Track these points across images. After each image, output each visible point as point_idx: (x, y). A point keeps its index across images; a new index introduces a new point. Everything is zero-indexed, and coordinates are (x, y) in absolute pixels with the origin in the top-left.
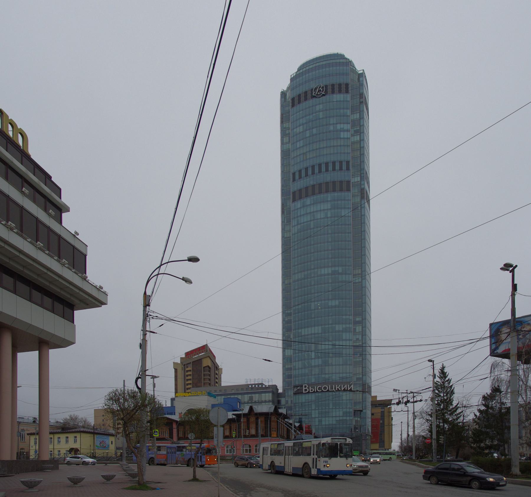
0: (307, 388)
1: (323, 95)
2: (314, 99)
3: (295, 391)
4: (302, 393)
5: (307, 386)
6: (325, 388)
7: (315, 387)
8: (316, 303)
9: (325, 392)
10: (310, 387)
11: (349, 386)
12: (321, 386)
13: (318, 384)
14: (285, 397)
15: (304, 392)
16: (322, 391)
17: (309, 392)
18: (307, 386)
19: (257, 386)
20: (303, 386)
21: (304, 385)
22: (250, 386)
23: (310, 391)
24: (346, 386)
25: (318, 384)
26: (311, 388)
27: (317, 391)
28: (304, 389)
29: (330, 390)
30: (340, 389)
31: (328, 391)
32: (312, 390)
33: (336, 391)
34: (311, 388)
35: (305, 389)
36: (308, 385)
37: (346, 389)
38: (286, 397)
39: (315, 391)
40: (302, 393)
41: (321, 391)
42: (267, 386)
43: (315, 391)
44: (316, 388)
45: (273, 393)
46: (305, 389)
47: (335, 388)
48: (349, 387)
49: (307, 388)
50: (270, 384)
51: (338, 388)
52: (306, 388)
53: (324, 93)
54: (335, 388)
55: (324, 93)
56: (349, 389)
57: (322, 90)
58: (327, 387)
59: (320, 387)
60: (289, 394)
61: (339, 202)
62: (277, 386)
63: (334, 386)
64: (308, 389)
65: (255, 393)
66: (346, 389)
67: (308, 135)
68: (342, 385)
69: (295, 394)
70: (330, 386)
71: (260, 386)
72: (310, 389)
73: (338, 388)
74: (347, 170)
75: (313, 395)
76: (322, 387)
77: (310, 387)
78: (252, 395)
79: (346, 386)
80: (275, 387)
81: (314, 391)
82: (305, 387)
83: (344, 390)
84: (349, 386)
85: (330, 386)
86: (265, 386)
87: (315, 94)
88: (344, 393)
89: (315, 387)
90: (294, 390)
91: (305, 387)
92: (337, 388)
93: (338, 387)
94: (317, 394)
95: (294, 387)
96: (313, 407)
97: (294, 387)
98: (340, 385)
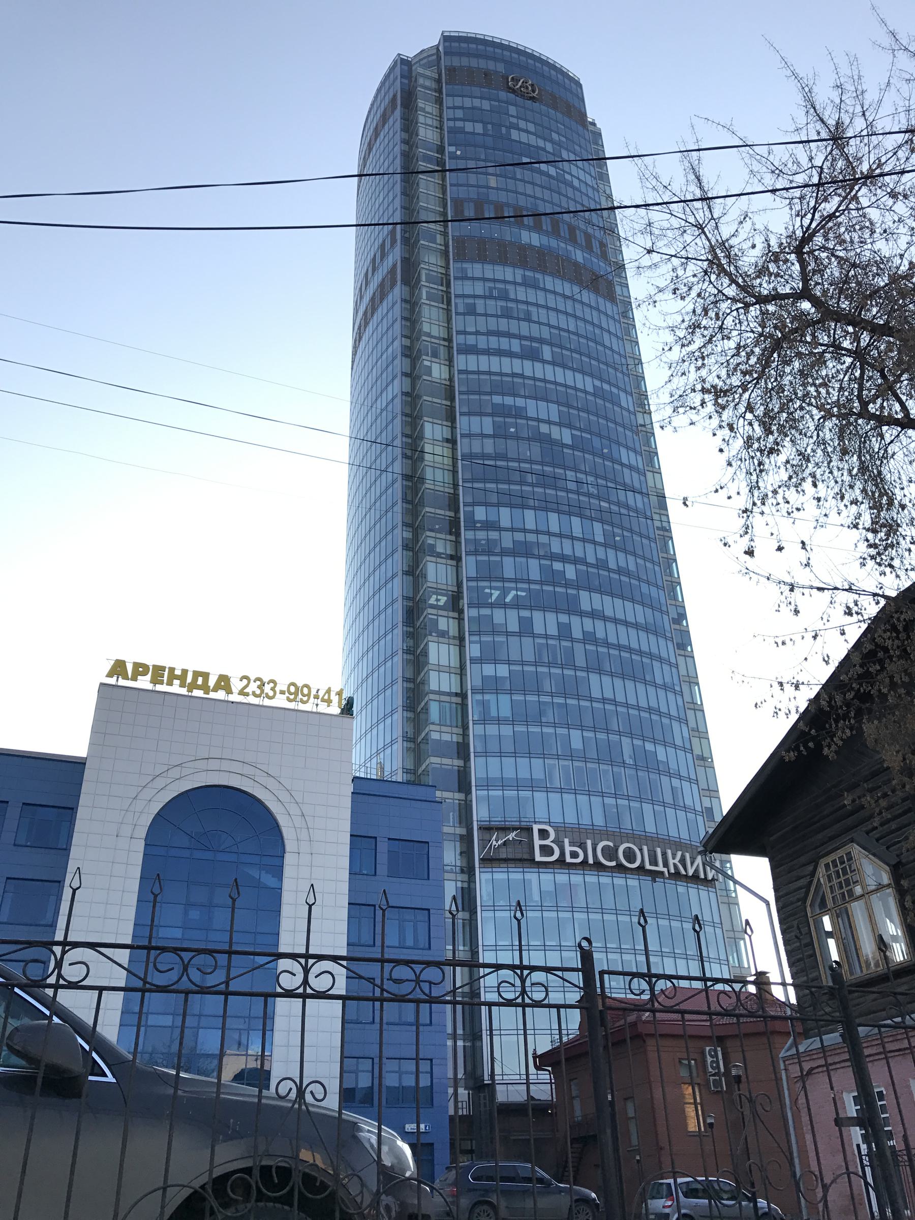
5: (552, 835)
7: (589, 843)
9: (631, 869)
10: (566, 841)
12: (611, 844)
15: (538, 858)
18: (552, 835)
21: (536, 828)
23: (569, 859)
28: (537, 842)
31: (641, 868)
32: (574, 855)
35: (541, 847)
39: (591, 861)
40: (530, 862)
41: (613, 864)
43: (591, 861)
44: (596, 850)
46: (541, 847)
47: (666, 864)
54: (666, 864)
63: (659, 851)
68: (688, 856)
70: (645, 848)
72: (568, 849)
77: (566, 841)
81: (585, 862)
82: (543, 834)
85: (645, 848)
89: (589, 843)
91: (543, 834)
92: (671, 862)
93: (674, 859)
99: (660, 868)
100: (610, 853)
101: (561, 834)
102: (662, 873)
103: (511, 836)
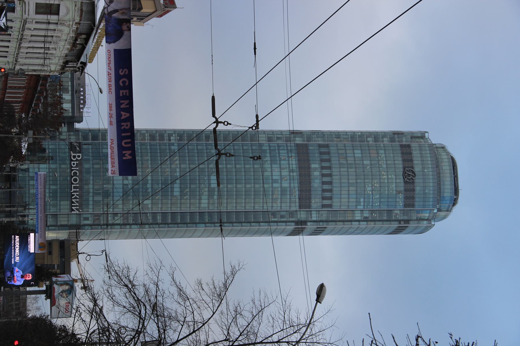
1: (404, 179)
2: (402, 170)
7: (77, 168)
10: (77, 162)
11: (78, 207)
12: (78, 175)
13: (80, 172)
14: (69, 131)
16: (72, 177)
19: (82, 97)
20: (80, 153)
21: (80, 155)
22: (82, 89)
23: (72, 162)
24: (77, 204)
29: (73, 185)
30: (73, 197)
34: (76, 163)
36: (80, 160)
37: (73, 205)
38: (68, 133)
39: (72, 168)
41: (72, 175)
42: (82, 110)
43: (72, 168)
45: (73, 117)
47: (74, 192)
48: (76, 208)
49: (77, 159)
50: (85, 114)
51: (75, 195)
53: (406, 181)
54: (74, 192)
55: (406, 181)
56: (73, 208)
57: (410, 178)
58: (77, 182)
59: (77, 173)
60: (72, 137)
61: (288, 197)
62: (82, 122)
63: (78, 190)
64: (75, 159)
65: (72, 96)
66: (73, 205)
67: (365, 162)
69: (71, 143)
71: (82, 102)
72: (75, 162)
73: (74, 195)
74: (323, 205)
75: (68, 166)
76: (77, 176)
77: (77, 162)
78: (70, 92)
79: (77, 204)
80: (80, 120)
82: (79, 156)
83: (73, 203)
84: (78, 207)
86: (83, 108)
87: (407, 170)
89: (77, 168)
90: (76, 142)
91: (79, 156)
92: (75, 194)
93: (77, 195)
94: (68, 170)
95: (80, 143)
98: (78, 197)
99: (73, 190)
101: (80, 161)
102: (71, 190)
103: (78, 148)
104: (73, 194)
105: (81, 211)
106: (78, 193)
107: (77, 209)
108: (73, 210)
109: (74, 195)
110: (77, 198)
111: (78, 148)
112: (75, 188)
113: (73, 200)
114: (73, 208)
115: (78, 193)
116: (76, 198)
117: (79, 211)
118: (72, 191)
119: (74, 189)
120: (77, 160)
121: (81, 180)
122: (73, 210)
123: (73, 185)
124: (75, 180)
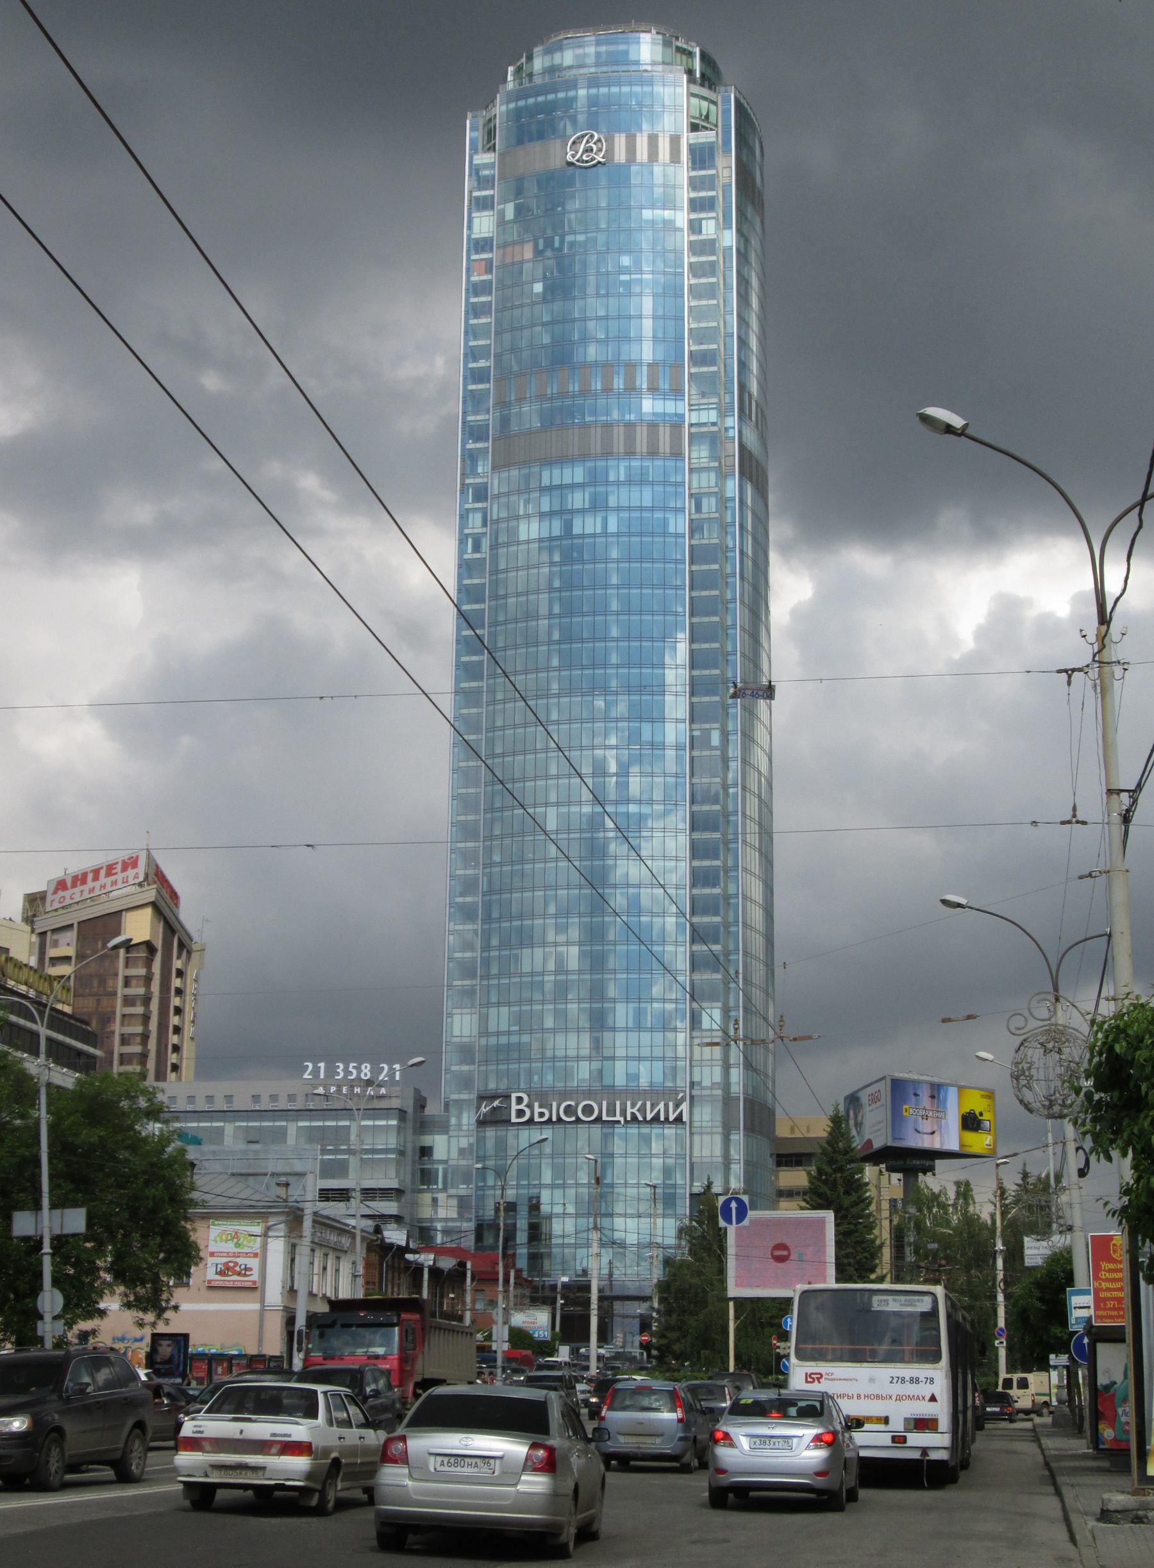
0: (527, 1106)
1: (599, 162)
3: (485, 1115)
4: (508, 1122)
5: (526, 1100)
6: (588, 1110)
7: (554, 1104)
8: (564, 810)
9: (589, 1122)
10: (536, 1104)
11: (671, 1105)
12: (573, 1103)
13: (564, 1095)
15: (514, 1120)
16: (578, 1120)
17: (531, 1121)
18: (526, 1100)
20: (510, 1096)
21: (514, 1096)
23: (537, 1119)
24: (661, 1106)
25: (564, 1095)
26: (540, 1107)
27: (560, 1120)
28: (514, 1107)
29: (605, 1118)
30: (640, 1118)
31: (598, 1119)
32: (541, 1115)
33: (626, 1121)
34: (540, 1107)
36: (529, 1095)
37: (662, 1119)
39: (554, 1119)
41: (573, 1119)
43: (554, 1119)
44: (557, 1109)
47: (623, 1113)
49: (527, 1106)
51: (634, 1110)
52: (521, 1107)
53: (603, 158)
54: (623, 1113)
55: (603, 158)
56: (672, 1118)
57: (595, 147)
59: (570, 1105)
63: (618, 1103)
66: (662, 1119)
68: (648, 1104)
70: (605, 1103)
72: (537, 1110)
73: (633, 1114)
76: (577, 1105)
77: (536, 1104)
79: (661, 1106)
81: (550, 1121)
82: (520, 1100)
83: (656, 1119)
84: (671, 1105)
85: (605, 1103)
87: (573, 156)
88: (656, 1130)
89: (554, 1104)
90: (478, 1107)
91: (520, 1100)
92: (629, 1111)
93: (633, 1106)
95: (481, 1098)
96: (547, 1178)
97: (481, 1098)
98: (640, 1103)
99: (618, 1118)
100: (569, 1110)
101: (533, 1097)
102: (618, 1122)
103: (496, 1103)
104: (629, 1118)
105: (681, 1095)
106: (629, 1103)
107: (677, 1106)
108: (679, 1119)
109: (633, 1114)
110: (644, 1105)
111: (496, 1103)
112: (611, 1111)
113: (649, 1117)
114: (671, 1118)
115: (629, 1103)
116: (642, 1110)
117: (683, 1100)
118: (622, 1120)
119: (615, 1116)
120: (530, 1106)
121: (589, 1094)
122: (679, 1119)
123: (605, 1118)
124: (588, 1110)
